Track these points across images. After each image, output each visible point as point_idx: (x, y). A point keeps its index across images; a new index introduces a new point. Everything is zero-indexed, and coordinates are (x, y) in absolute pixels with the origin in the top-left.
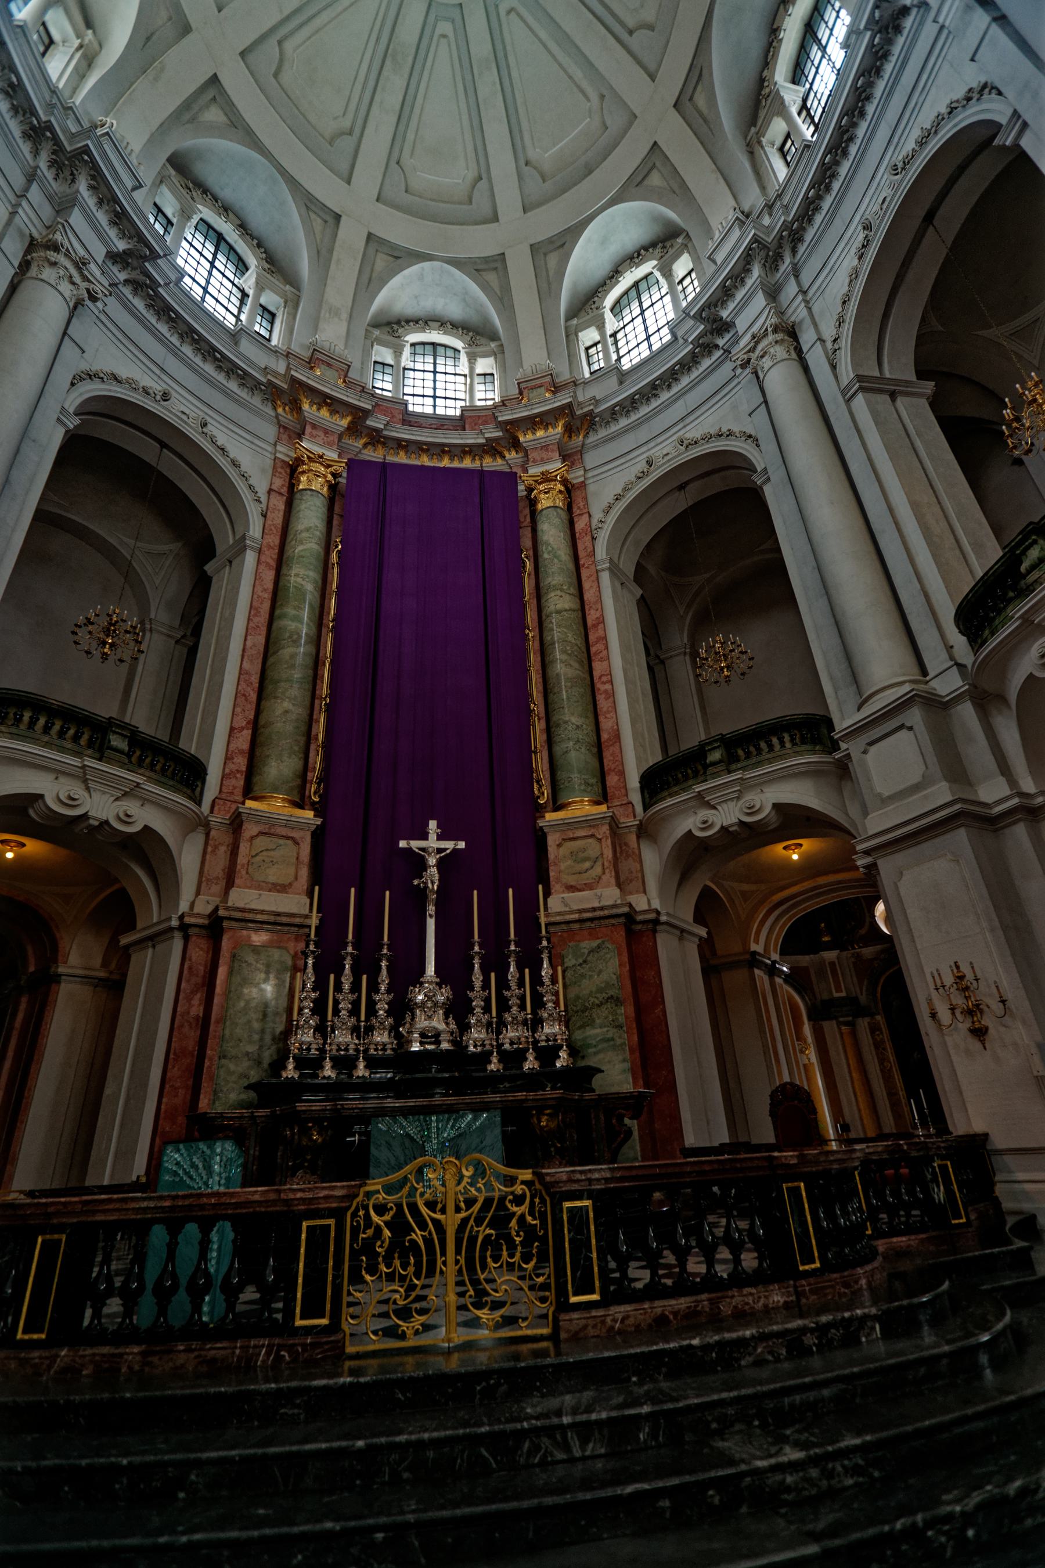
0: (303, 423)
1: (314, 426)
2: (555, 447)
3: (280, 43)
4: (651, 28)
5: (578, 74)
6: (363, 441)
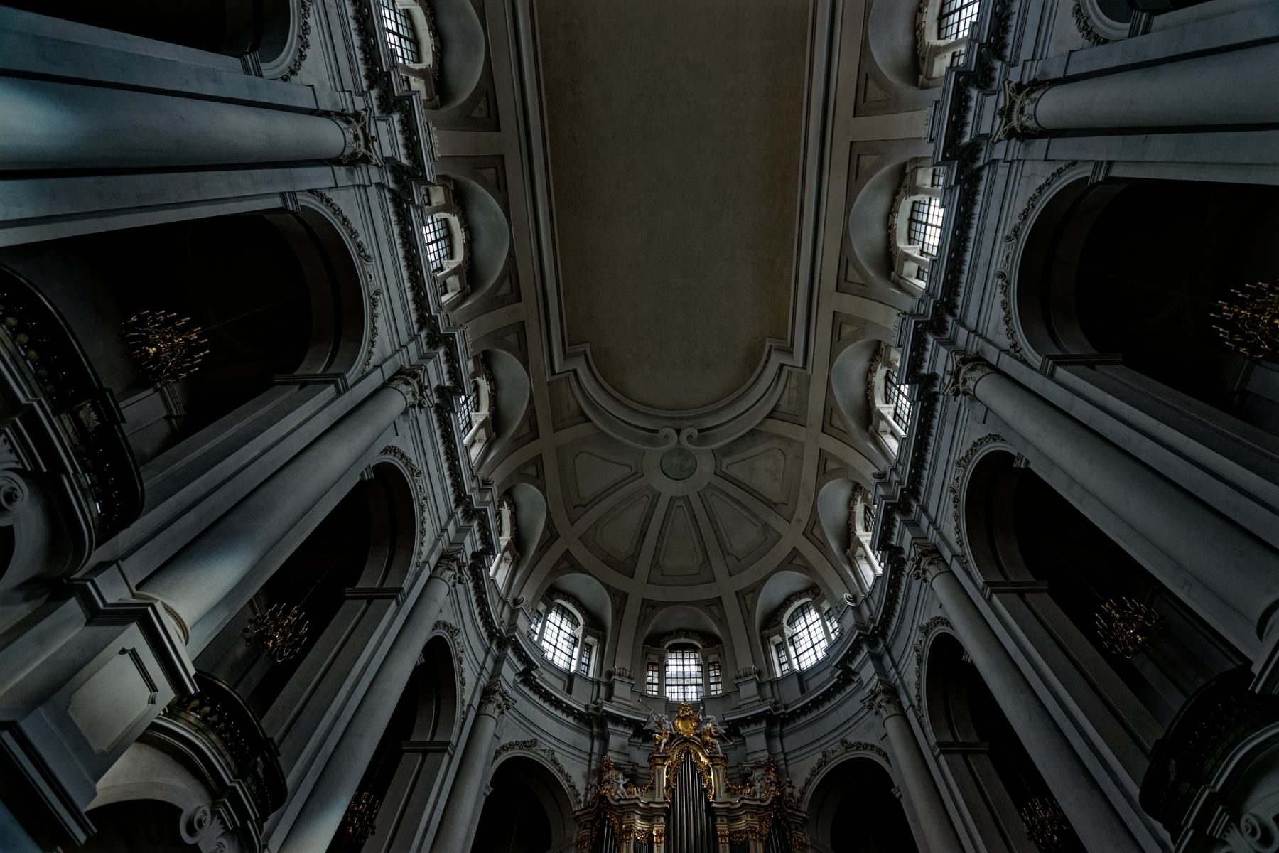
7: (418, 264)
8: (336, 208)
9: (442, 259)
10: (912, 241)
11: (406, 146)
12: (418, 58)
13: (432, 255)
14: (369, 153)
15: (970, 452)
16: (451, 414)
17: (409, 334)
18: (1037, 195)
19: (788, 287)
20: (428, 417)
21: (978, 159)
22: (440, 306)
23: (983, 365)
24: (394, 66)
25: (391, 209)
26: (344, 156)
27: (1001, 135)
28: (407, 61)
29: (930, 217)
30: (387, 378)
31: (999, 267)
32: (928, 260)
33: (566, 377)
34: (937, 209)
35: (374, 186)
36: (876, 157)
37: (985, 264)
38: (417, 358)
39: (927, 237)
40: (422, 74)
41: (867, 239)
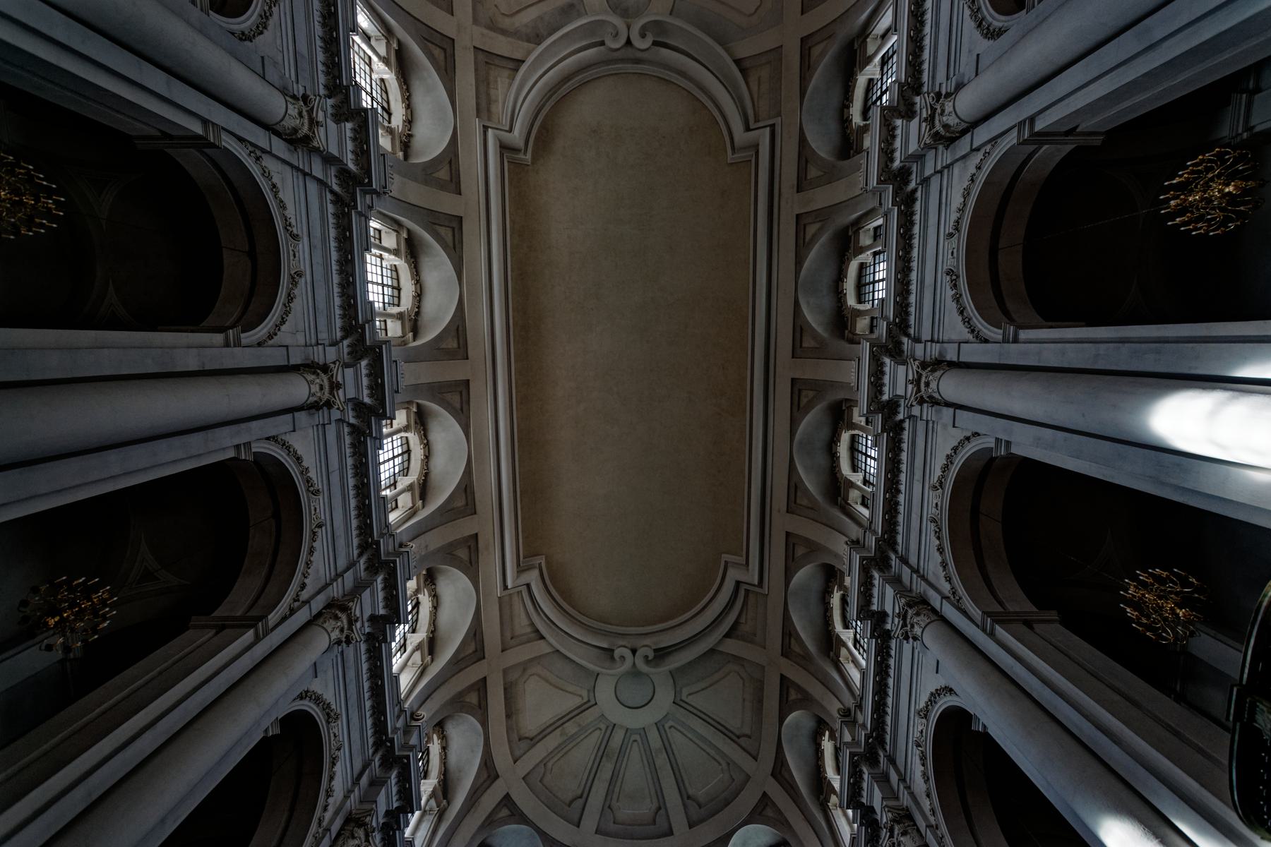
5: (713, 752)
7: (900, 263)
8: (966, 324)
9: (872, 264)
10: (393, 269)
11: (883, 373)
13: (881, 269)
14: (919, 370)
15: (268, 14)
16: (903, 81)
17: (928, 186)
20: (934, 77)
21: (348, 346)
22: (886, 215)
23: (286, 134)
25: (912, 318)
26: (943, 369)
28: (865, 436)
29: (381, 292)
30: (969, 134)
31: (301, 246)
32: (374, 251)
33: (759, 121)
36: (443, 346)
37: (315, 247)
38: (927, 157)
39: (379, 272)
40: (852, 426)
41: (438, 268)
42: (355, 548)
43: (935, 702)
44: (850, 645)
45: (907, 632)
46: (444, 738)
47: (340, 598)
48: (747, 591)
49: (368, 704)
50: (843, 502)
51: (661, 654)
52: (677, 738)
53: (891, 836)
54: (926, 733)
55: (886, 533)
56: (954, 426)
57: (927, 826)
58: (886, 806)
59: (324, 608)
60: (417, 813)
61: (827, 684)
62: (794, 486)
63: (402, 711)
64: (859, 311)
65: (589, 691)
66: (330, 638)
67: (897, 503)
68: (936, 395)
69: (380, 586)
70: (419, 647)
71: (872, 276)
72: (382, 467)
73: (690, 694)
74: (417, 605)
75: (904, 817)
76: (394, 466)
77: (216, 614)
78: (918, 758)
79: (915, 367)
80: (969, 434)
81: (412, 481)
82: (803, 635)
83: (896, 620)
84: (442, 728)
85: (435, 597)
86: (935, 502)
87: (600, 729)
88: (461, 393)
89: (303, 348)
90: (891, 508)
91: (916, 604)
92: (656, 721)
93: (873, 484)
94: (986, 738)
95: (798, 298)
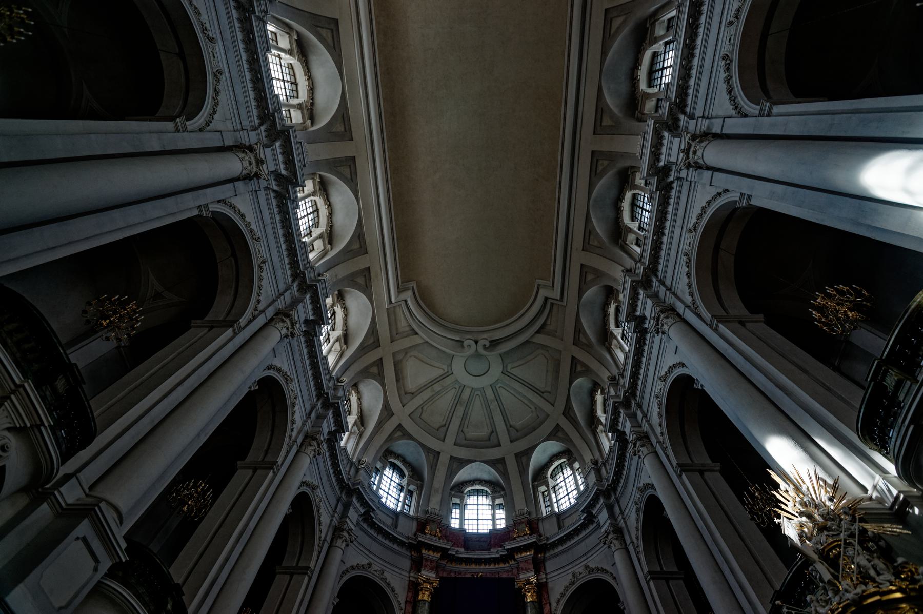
0: (421, 557)
1: (426, 560)
2: (531, 561)
3: (422, 408)
4: (550, 393)
5: (526, 401)
6: (446, 561)
7: (686, 51)
8: (732, 102)
9: (663, 52)
10: (290, 67)
11: (662, 144)
12: (634, 197)
13: (670, 56)
18: (215, 107)
19: (378, 23)
24: (652, 194)
27: (258, 148)
28: (643, 194)
29: (283, 87)
31: (217, 47)
34: (280, 93)
35: (697, 115)
36: (334, 130)
40: (635, 187)
42: (289, 277)
43: (672, 372)
44: (619, 338)
45: (658, 329)
46: (358, 393)
47: (284, 309)
48: (552, 304)
49: (310, 373)
50: (623, 243)
51: (494, 344)
52: (503, 393)
53: (635, 447)
54: (664, 390)
55: (651, 264)
56: (710, 185)
57: (657, 442)
58: (633, 431)
59: (275, 315)
60: (347, 434)
61: (601, 361)
62: (589, 232)
63: (331, 377)
64: (648, 94)
65: (448, 366)
66: (281, 333)
67: (661, 243)
68: (700, 161)
69: (308, 302)
70: (338, 340)
71: (662, 63)
72: (300, 221)
73: (513, 368)
74: (334, 314)
75: (644, 438)
76: (309, 221)
77: (207, 319)
78: (656, 405)
79: (687, 139)
80: (720, 190)
81: (322, 231)
82: (588, 332)
83: (652, 321)
84: (357, 387)
85: (345, 309)
86: (689, 241)
87: (455, 388)
88: (350, 166)
89: (232, 133)
90: (657, 246)
91: (666, 311)
92: (491, 383)
93: (646, 230)
94: (703, 393)
95: (601, 85)
